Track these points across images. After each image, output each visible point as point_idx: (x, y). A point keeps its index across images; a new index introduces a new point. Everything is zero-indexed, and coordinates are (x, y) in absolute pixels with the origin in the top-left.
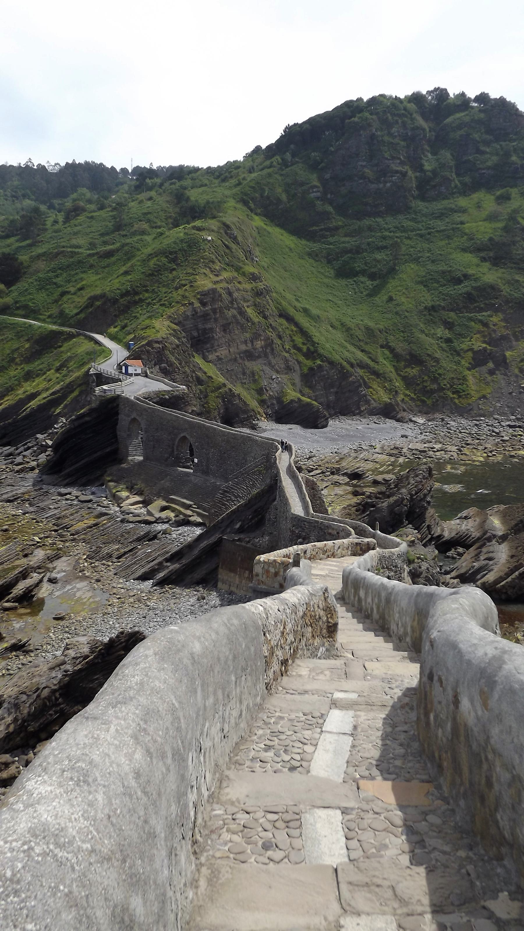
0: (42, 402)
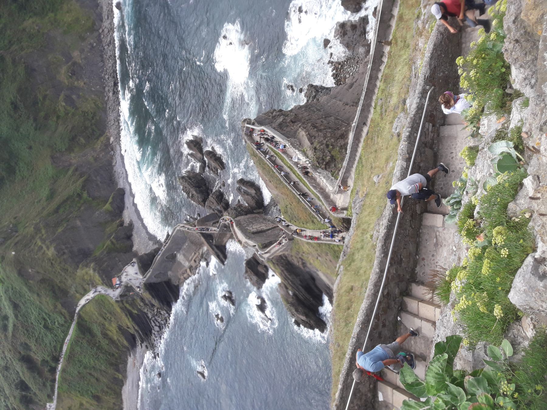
0: (130, 319)
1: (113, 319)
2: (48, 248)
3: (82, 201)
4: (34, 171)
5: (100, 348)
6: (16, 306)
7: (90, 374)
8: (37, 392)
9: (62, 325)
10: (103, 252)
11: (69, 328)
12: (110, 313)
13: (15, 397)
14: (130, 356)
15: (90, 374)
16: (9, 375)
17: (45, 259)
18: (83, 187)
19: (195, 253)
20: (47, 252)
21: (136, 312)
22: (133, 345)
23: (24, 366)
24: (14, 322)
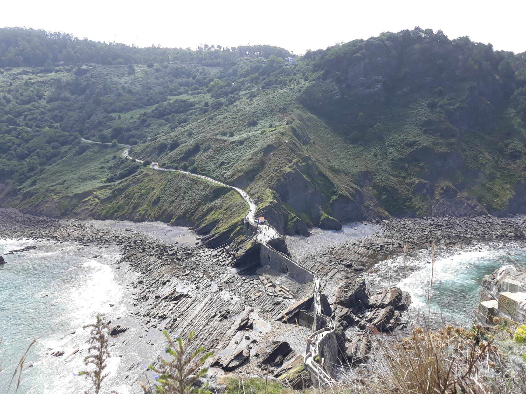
0: (225, 230)
1: (225, 216)
2: (290, 167)
3: (329, 194)
4: (354, 157)
5: (200, 204)
6: (241, 142)
7: (178, 196)
8: (169, 156)
9: (223, 176)
10: (285, 210)
11: (220, 181)
12: (231, 214)
13: (166, 139)
14: (190, 229)
15: (178, 196)
16: (184, 136)
17: (281, 165)
18: (341, 196)
19: (288, 291)
20: (287, 166)
21: (232, 235)
22: (199, 233)
23: (191, 147)
24: (228, 140)
